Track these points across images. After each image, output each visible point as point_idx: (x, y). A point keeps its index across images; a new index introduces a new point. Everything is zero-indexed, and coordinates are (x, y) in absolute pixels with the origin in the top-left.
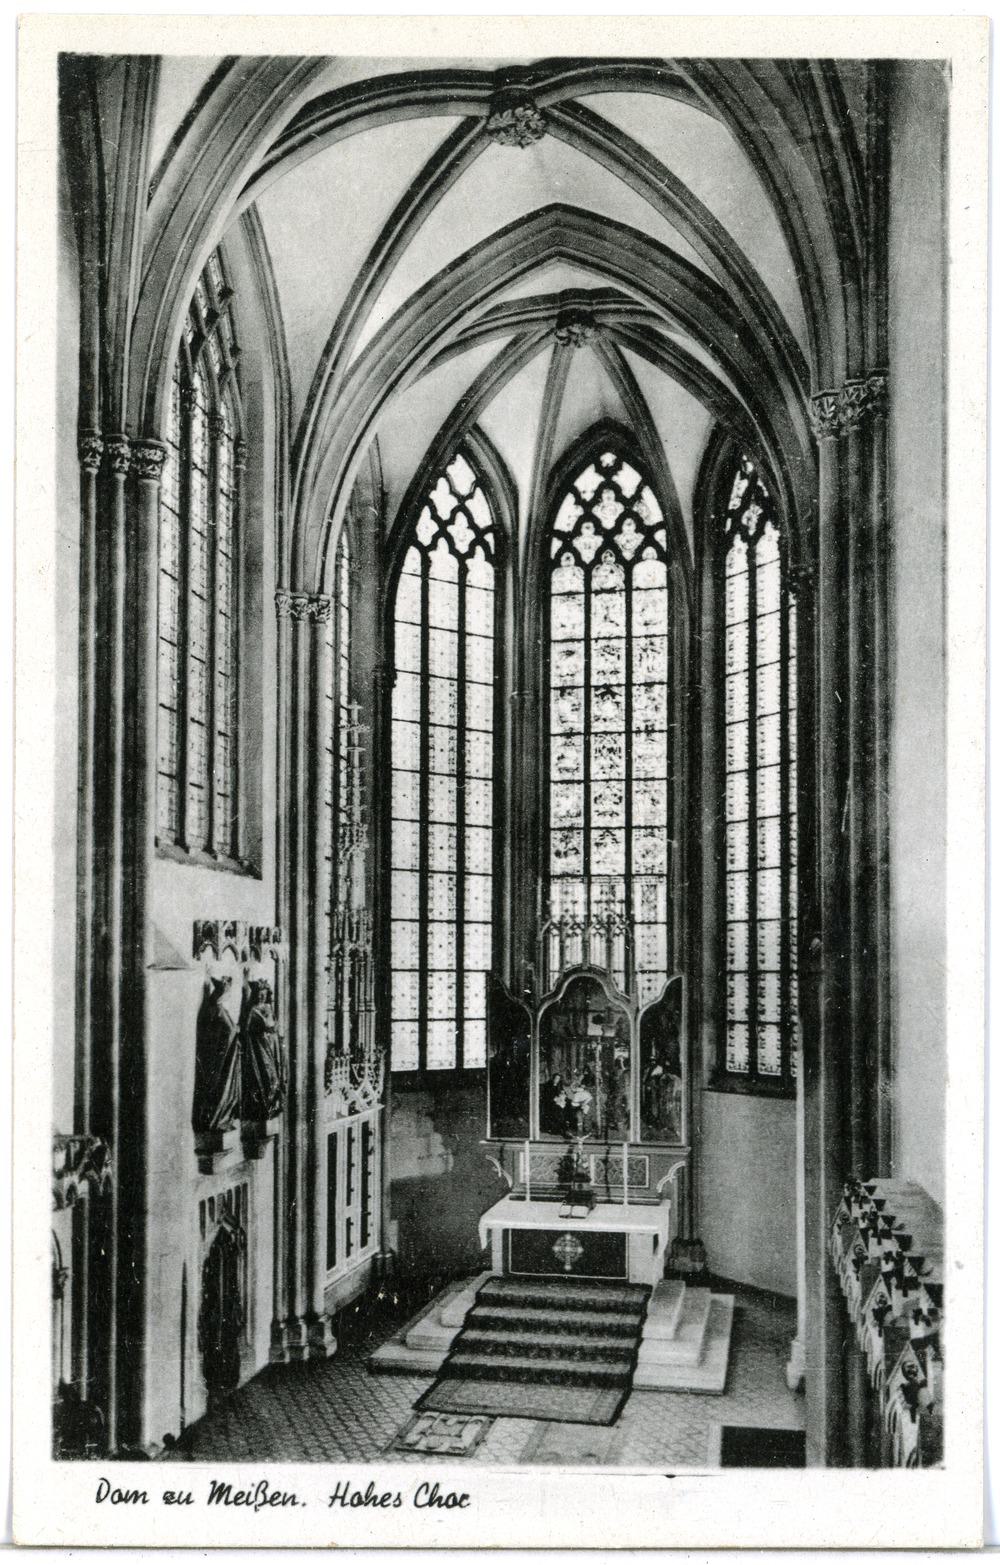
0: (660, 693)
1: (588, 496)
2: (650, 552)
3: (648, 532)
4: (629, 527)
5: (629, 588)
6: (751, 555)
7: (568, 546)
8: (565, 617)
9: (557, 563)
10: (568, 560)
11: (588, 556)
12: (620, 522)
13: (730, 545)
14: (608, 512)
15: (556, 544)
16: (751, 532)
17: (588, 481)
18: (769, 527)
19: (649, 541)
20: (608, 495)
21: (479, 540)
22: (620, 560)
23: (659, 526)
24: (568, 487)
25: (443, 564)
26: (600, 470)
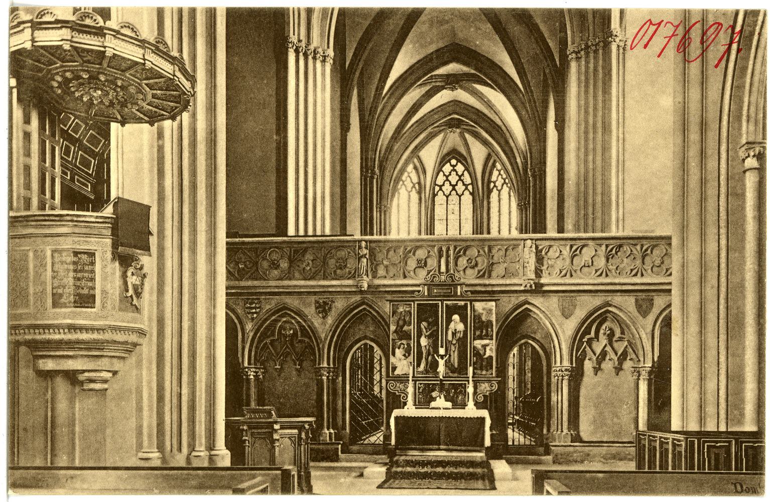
1: (447, 174)
2: (467, 193)
3: (466, 186)
4: (460, 183)
7: (441, 189)
8: (440, 211)
9: (437, 195)
10: (440, 193)
14: (454, 179)
15: (437, 188)
17: (447, 168)
19: (466, 189)
20: (454, 173)
21: (414, 186)
22: (457, 194)
24: (440, 170)
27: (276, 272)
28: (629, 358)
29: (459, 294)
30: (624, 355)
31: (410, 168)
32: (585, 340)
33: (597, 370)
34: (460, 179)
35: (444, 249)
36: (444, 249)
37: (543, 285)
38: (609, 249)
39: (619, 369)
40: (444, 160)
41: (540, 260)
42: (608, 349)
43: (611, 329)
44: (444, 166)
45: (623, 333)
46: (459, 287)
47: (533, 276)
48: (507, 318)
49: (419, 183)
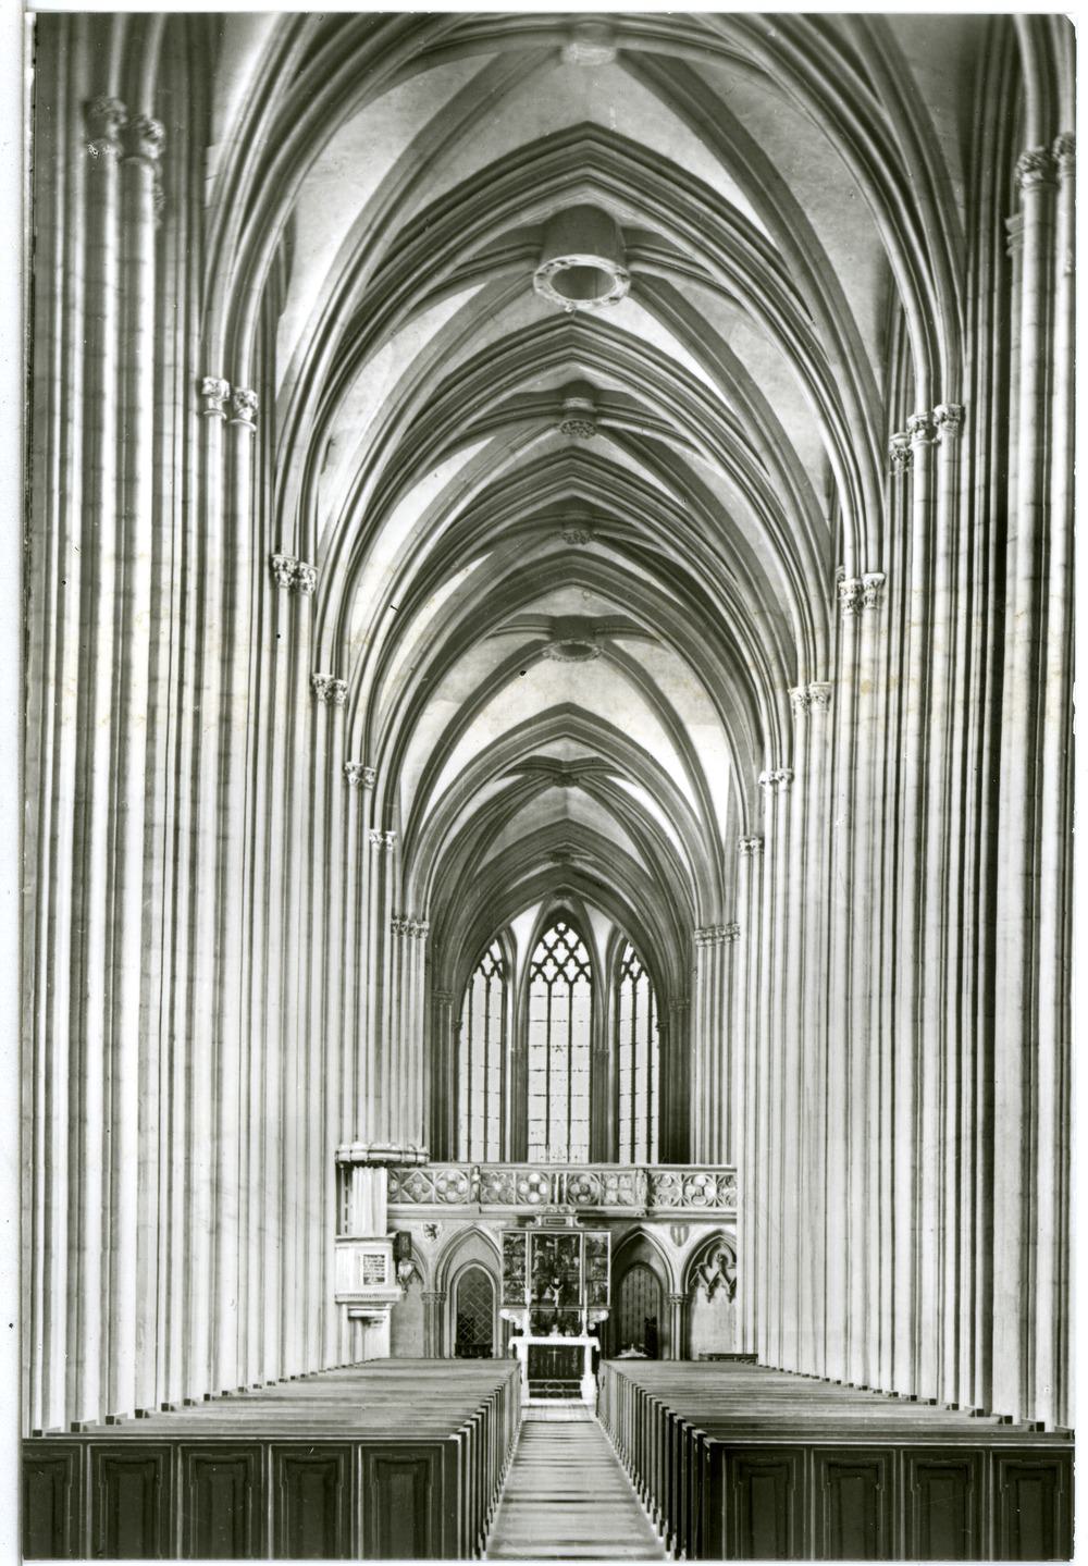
0: (587, 1051)
1: (550, 945)
2: (582, 978)
3: (582, 967)
4: (572, 962)
5: (571, 996)
6: (634, 987)
7: (539, 971)
8: (537, 1008)
9: (533, 979)
10: (539, 978)
11: (550, 978)
12: (567, 959)
13: (623, 980)
14: (561, 954)
16: (635, 975)
17: (551, 937)
18: (643, 974)
19: (582, 971)
20: (561, 945)
21: (495, 968)
22: (566, 980)
23: (587, 964)
24: (540, 939)
25: (478, 977)
26: (557, 931)
32: (697, 1267)
33: (711, 1296)
34: (571, 956)
37: (655, 1213)
40: (546, 923)
42: (721, 1276)
43: (724, 1258)
44: (545, 931)
47: (645, 1206)
48: (620, 1245)
49: (504, 960)
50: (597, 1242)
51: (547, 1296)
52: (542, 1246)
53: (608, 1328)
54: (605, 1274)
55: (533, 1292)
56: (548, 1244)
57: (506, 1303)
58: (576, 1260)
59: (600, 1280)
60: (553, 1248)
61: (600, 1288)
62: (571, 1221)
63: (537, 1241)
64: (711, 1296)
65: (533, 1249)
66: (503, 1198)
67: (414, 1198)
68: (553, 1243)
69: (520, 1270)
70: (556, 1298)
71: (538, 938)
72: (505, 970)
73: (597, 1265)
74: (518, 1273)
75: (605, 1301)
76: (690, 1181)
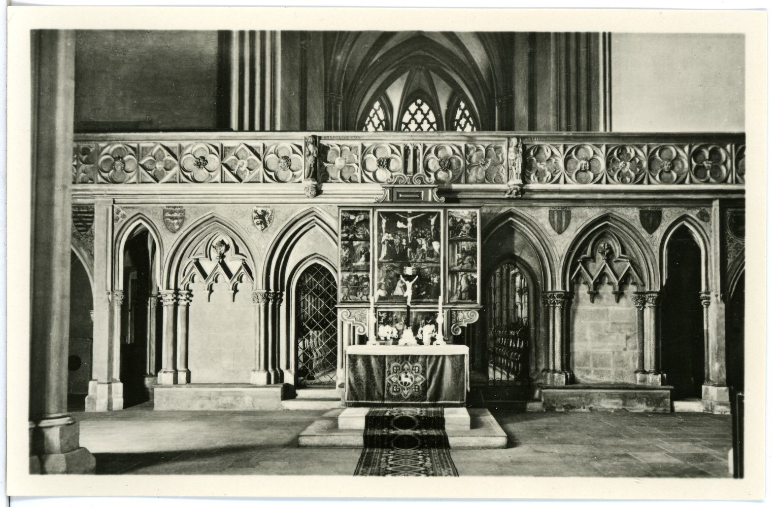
1: (413, 112)
3: (431, 124)
4: (425, 121)
7: (407, 127)
12: (423, 120)
14: (419, 117)
15: (403, 126)
16: (463, 126)
17: (413, 108)
19: (431, 127)
20: (419, 112)
21: (381, 124)
26: (417, 104)
27: (201, 174)
28: (631, 281)
29: (430, 199)
30: (628, 275)
31: (377, 105)
33: (594, 295)
34: (425, 118)
35: (411, 148)
36: (411, 148)
38: (610, 151)
39: (619, 295)
41: (527, 165)
42: (608, 271)
44: (410, 104)
45: (624, 251)
46: (430, 191)
50: (462, 221)
51: (398, 291)
52: (391, 228)
53: (474, 333)
54: (473, 263)
55: (380, 287)
56: (400, 225)
57: (343, 302)
58: (435, 245)
59: (466, 271)
60: (405, 230)
61: (468, 281)
62: (431, 195)
63: (384, 221)
64: (594, 295)
65: (380, 230)
66: (346, 176)
67: (237, 176)
68: (406, 223)
69: (363, 258)
70: (409, 293)
71: (404, 108)
72: (397, 183)
73: (463, 251)
74: (361, 262)
75: (473, 297)
76: (573, 153)
